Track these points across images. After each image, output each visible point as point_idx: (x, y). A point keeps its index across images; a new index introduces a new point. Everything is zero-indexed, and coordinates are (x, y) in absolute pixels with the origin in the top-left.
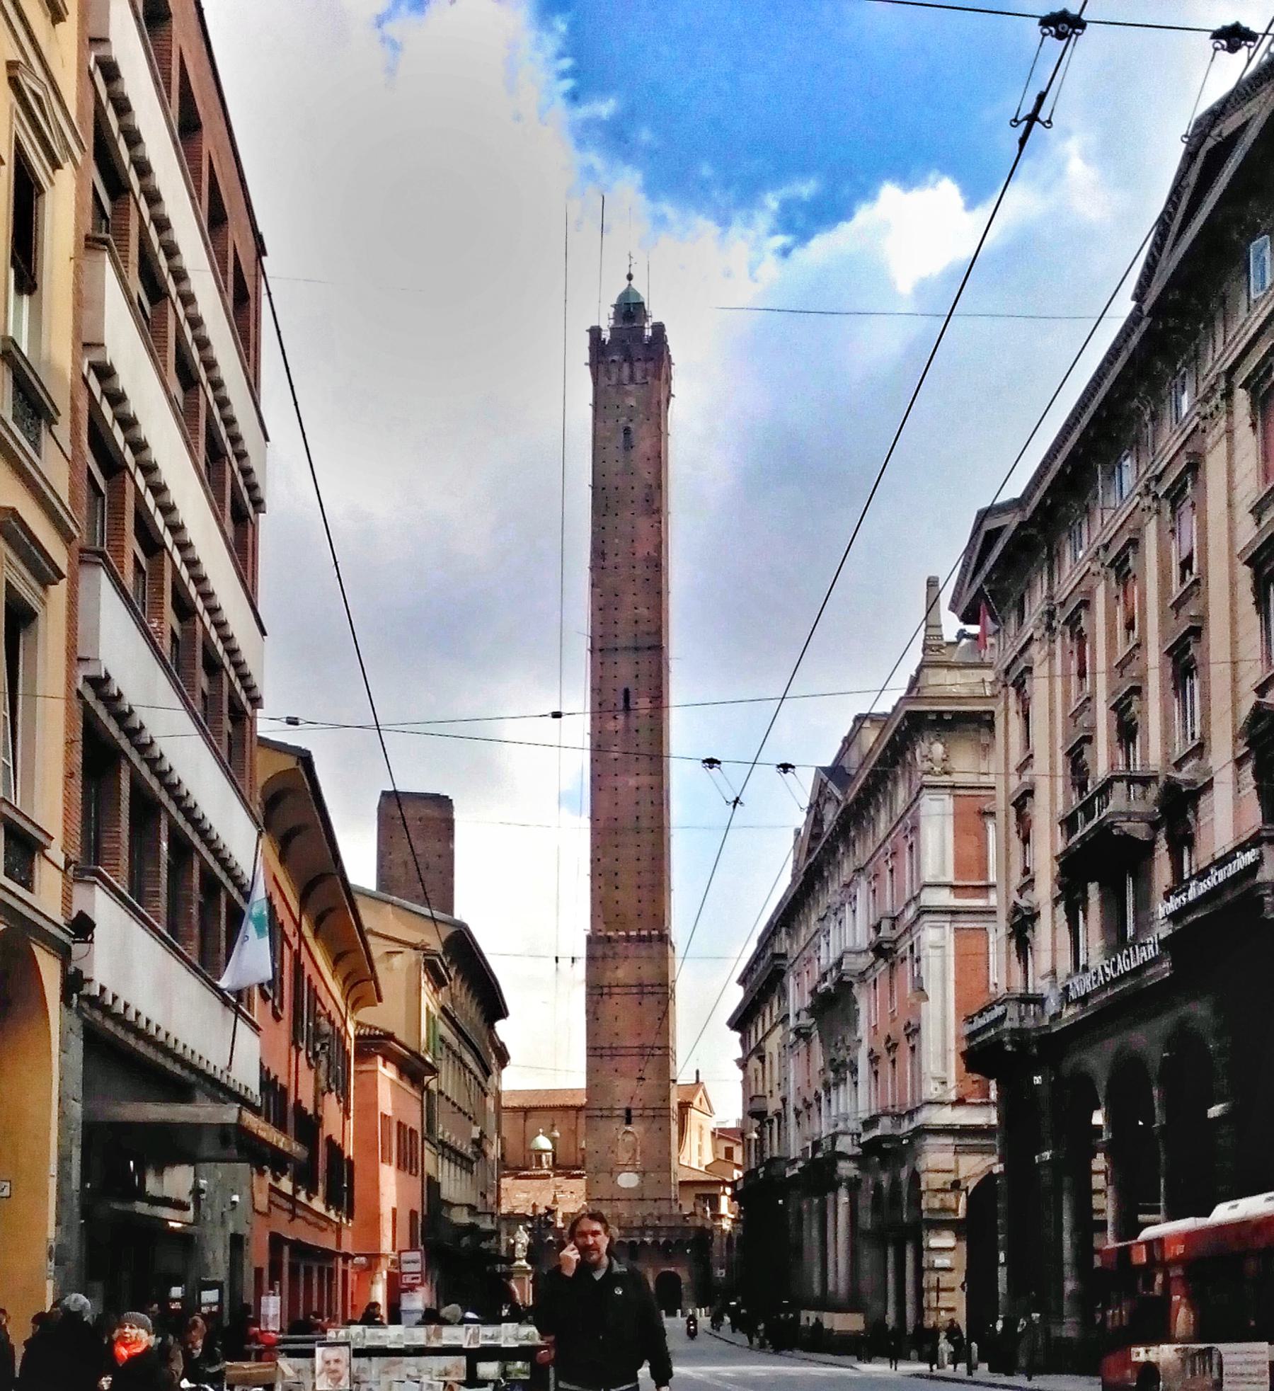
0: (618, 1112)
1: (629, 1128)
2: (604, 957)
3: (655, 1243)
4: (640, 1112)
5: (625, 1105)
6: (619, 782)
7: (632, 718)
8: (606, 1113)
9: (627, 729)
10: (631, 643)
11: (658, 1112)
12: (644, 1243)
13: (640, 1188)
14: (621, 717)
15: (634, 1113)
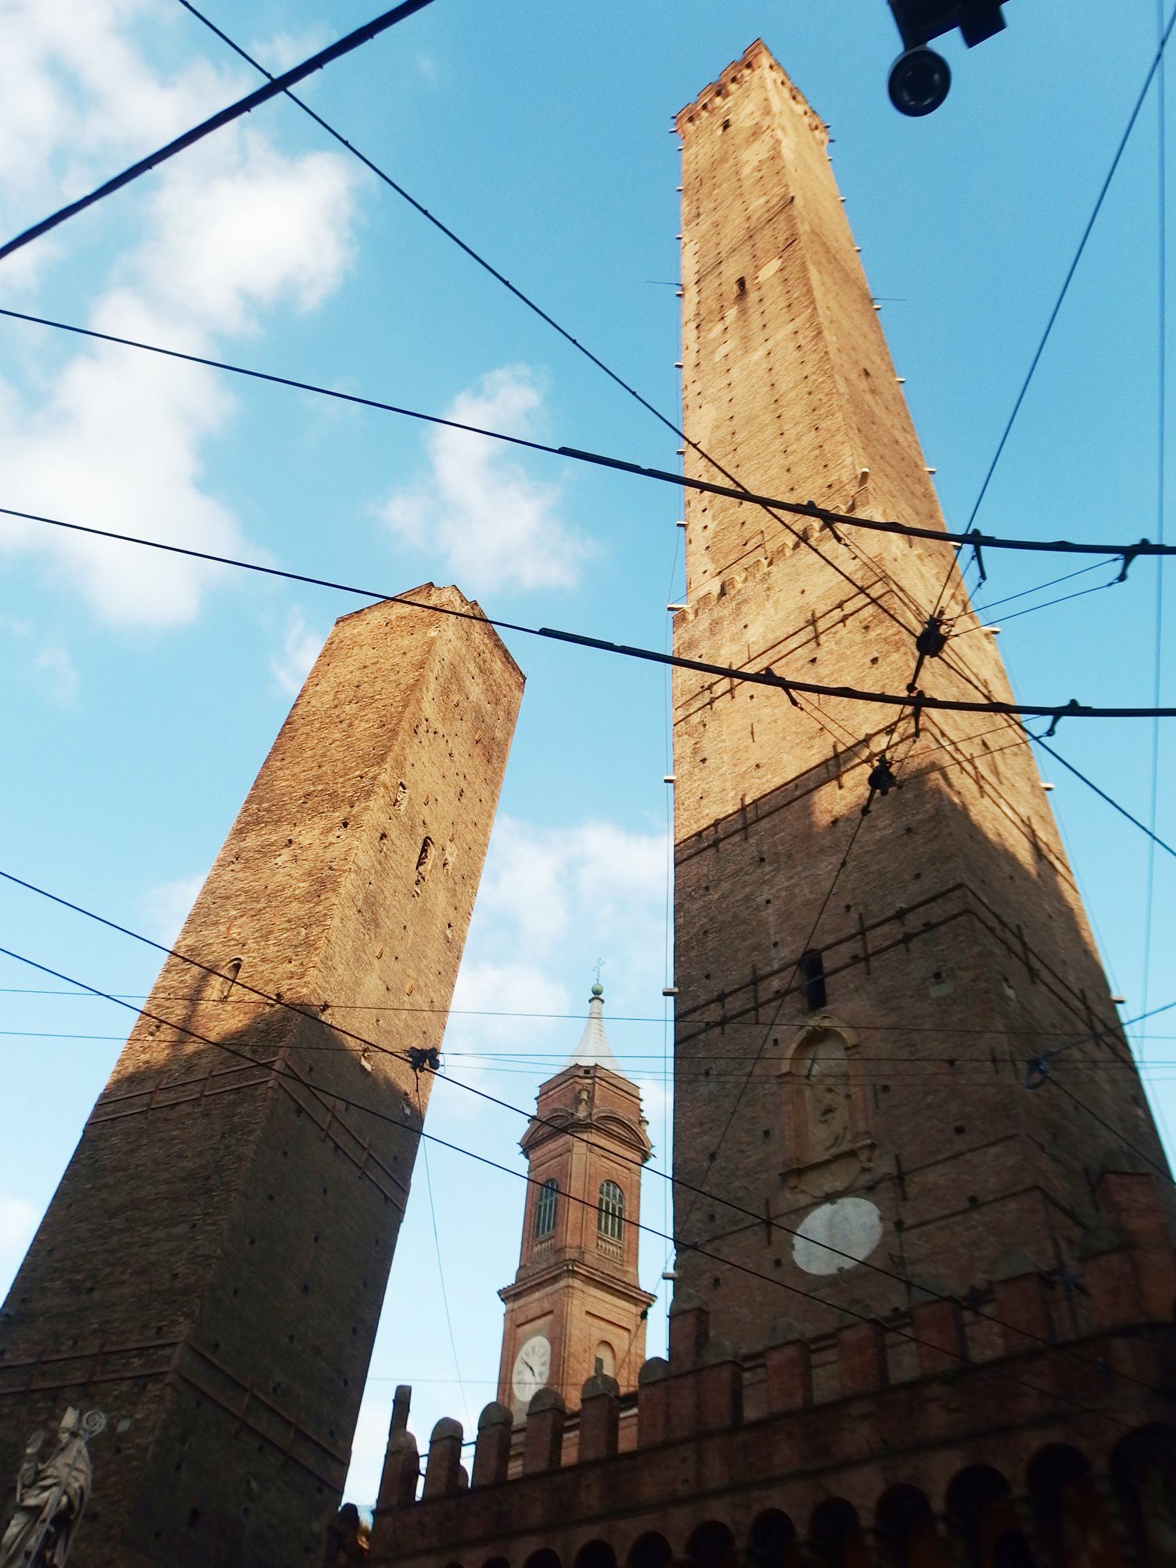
0: (776, 984)
1: (814, 1022)
2: (715, 627)
3: (902, 1503)
4: (854, 947)
5: (791, 950)
6: (735, 373)
7: (753, 297)
8: (734, 1004)
9: (743, 312)
10: (741, 234)
11: (914, 922)
12: (834, 1515)
13: (887, 1264)
14: (732, 313)
15: (829, 962)
